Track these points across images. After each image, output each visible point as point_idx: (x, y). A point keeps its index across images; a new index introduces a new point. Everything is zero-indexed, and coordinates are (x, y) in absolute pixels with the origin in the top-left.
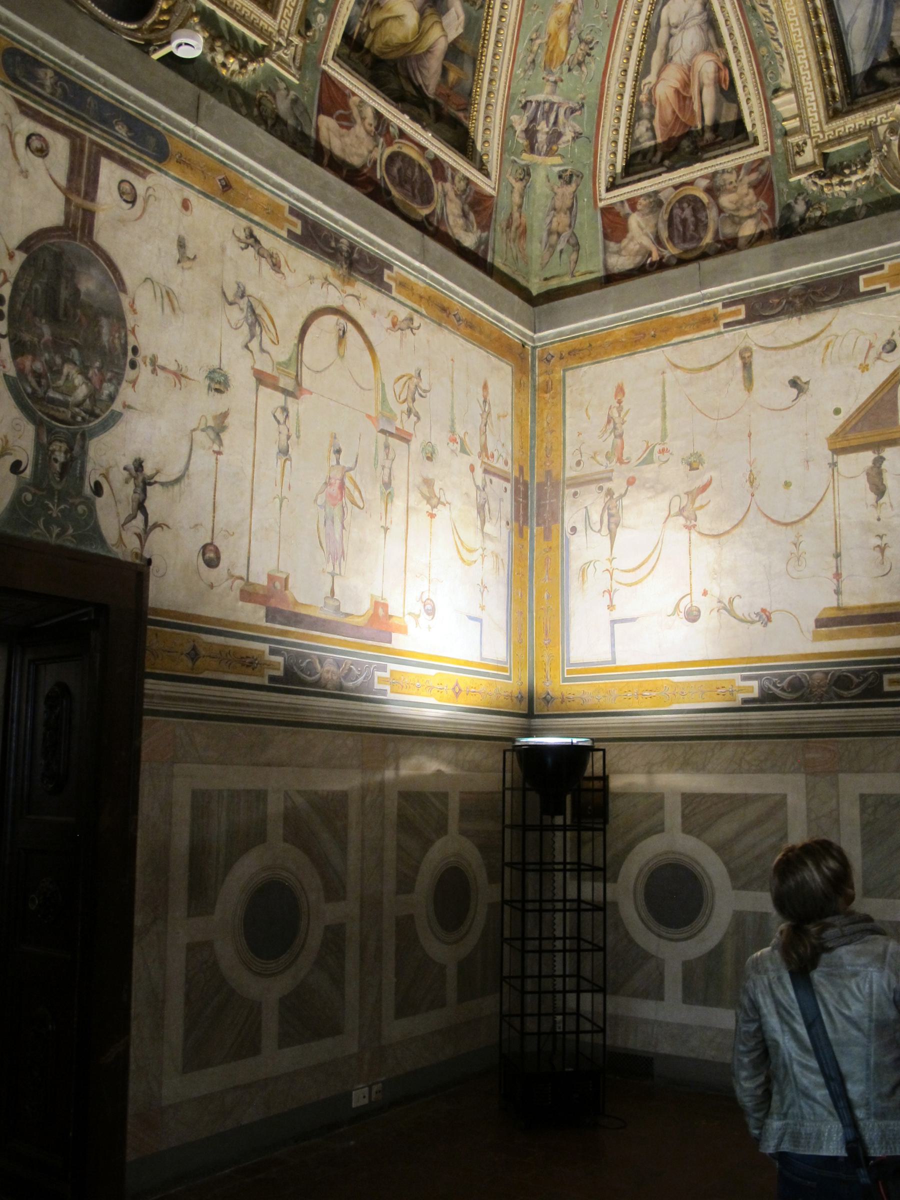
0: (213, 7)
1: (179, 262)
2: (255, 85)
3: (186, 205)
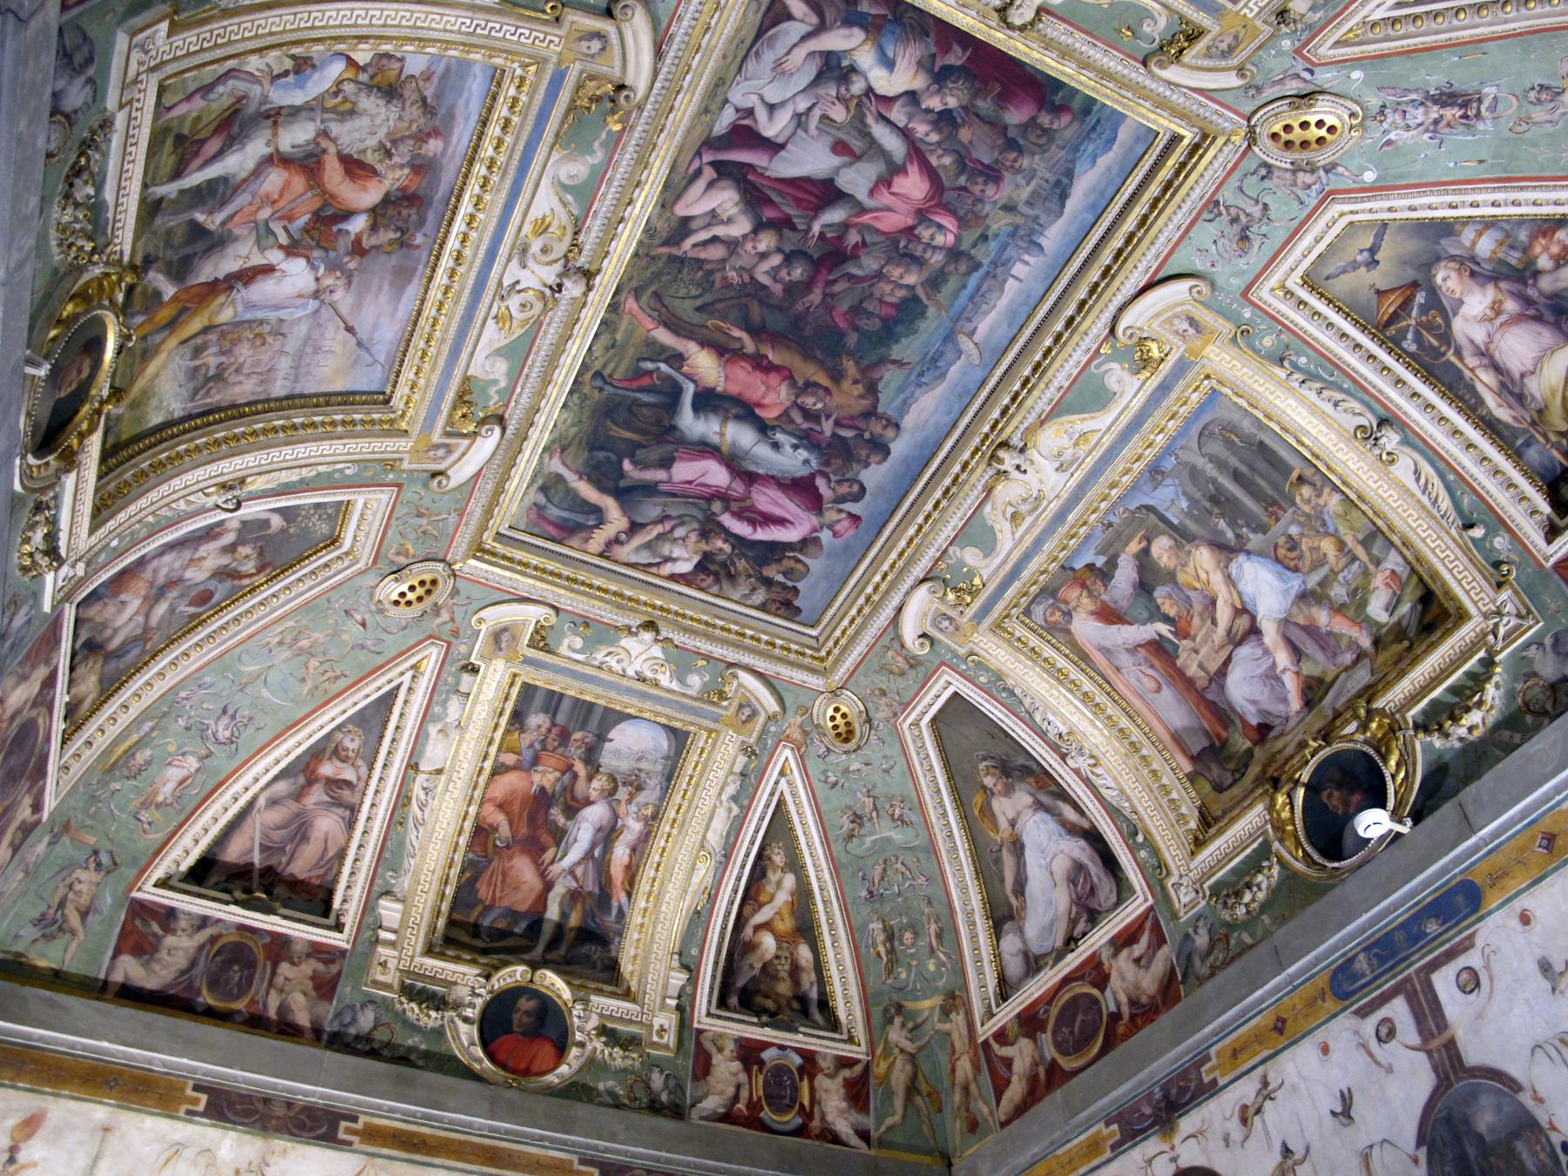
0: (1426, 701)
1: (1554, 990)
2: (1510, 695)
3: (1525, 919)
